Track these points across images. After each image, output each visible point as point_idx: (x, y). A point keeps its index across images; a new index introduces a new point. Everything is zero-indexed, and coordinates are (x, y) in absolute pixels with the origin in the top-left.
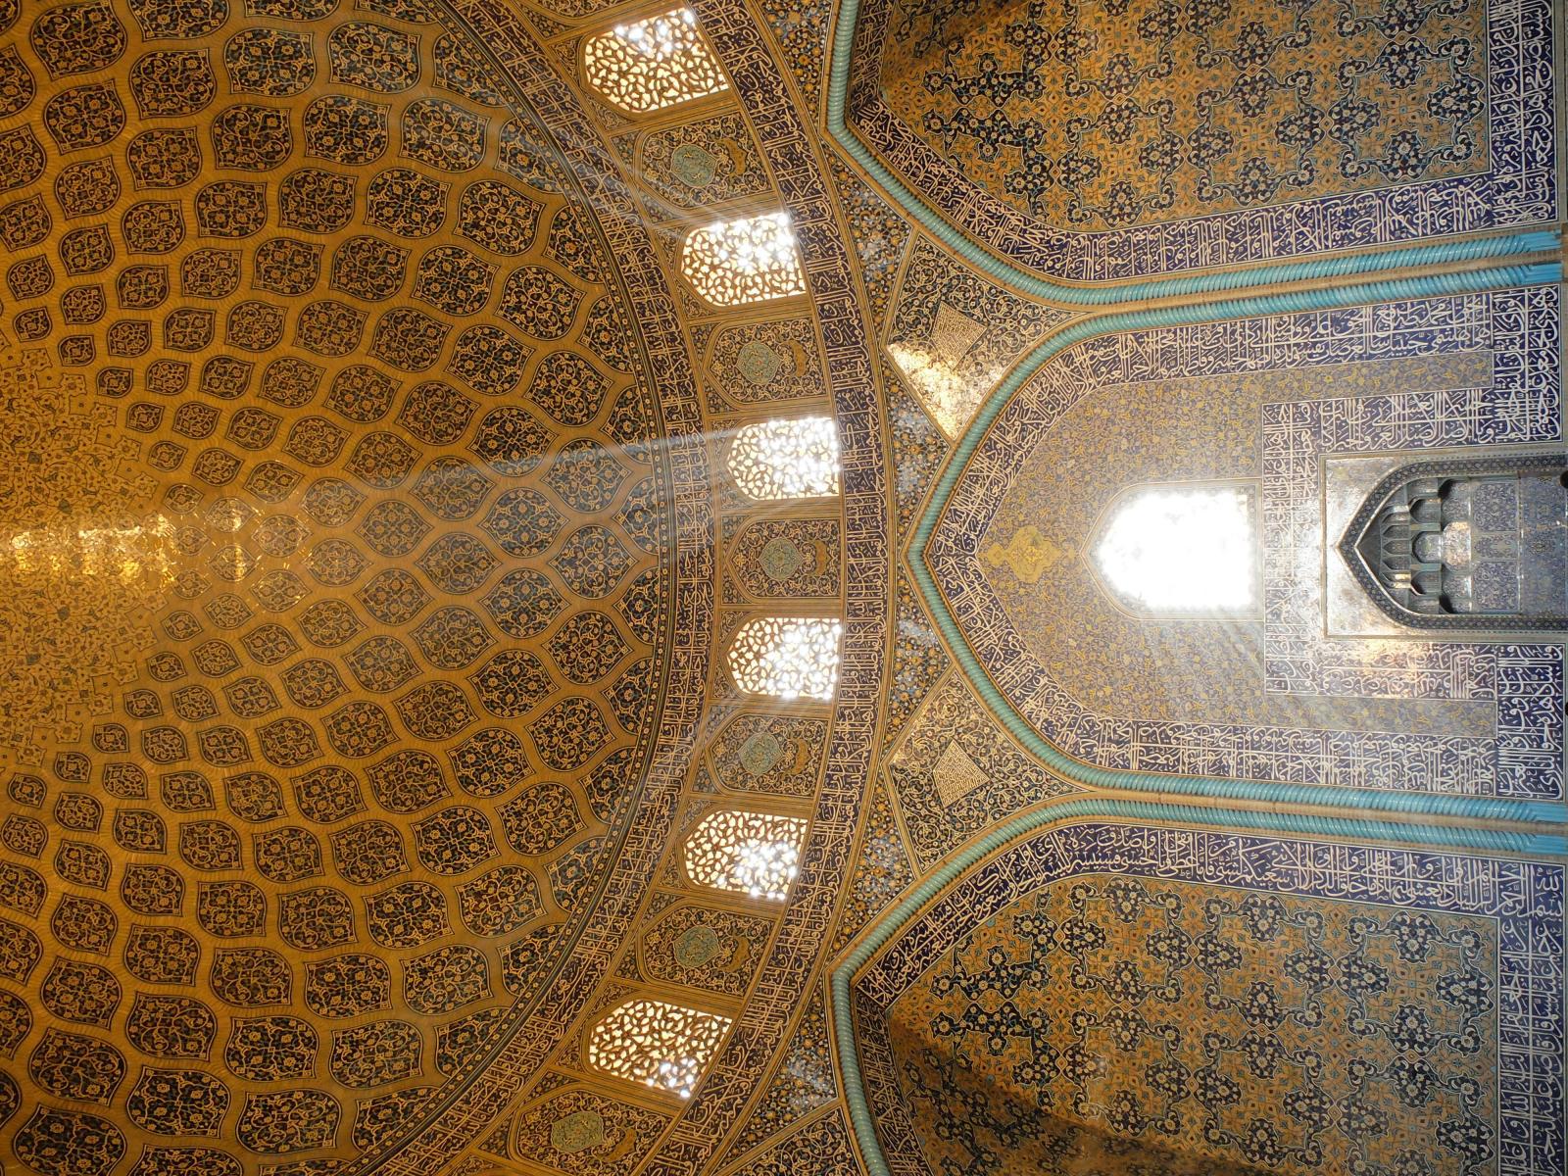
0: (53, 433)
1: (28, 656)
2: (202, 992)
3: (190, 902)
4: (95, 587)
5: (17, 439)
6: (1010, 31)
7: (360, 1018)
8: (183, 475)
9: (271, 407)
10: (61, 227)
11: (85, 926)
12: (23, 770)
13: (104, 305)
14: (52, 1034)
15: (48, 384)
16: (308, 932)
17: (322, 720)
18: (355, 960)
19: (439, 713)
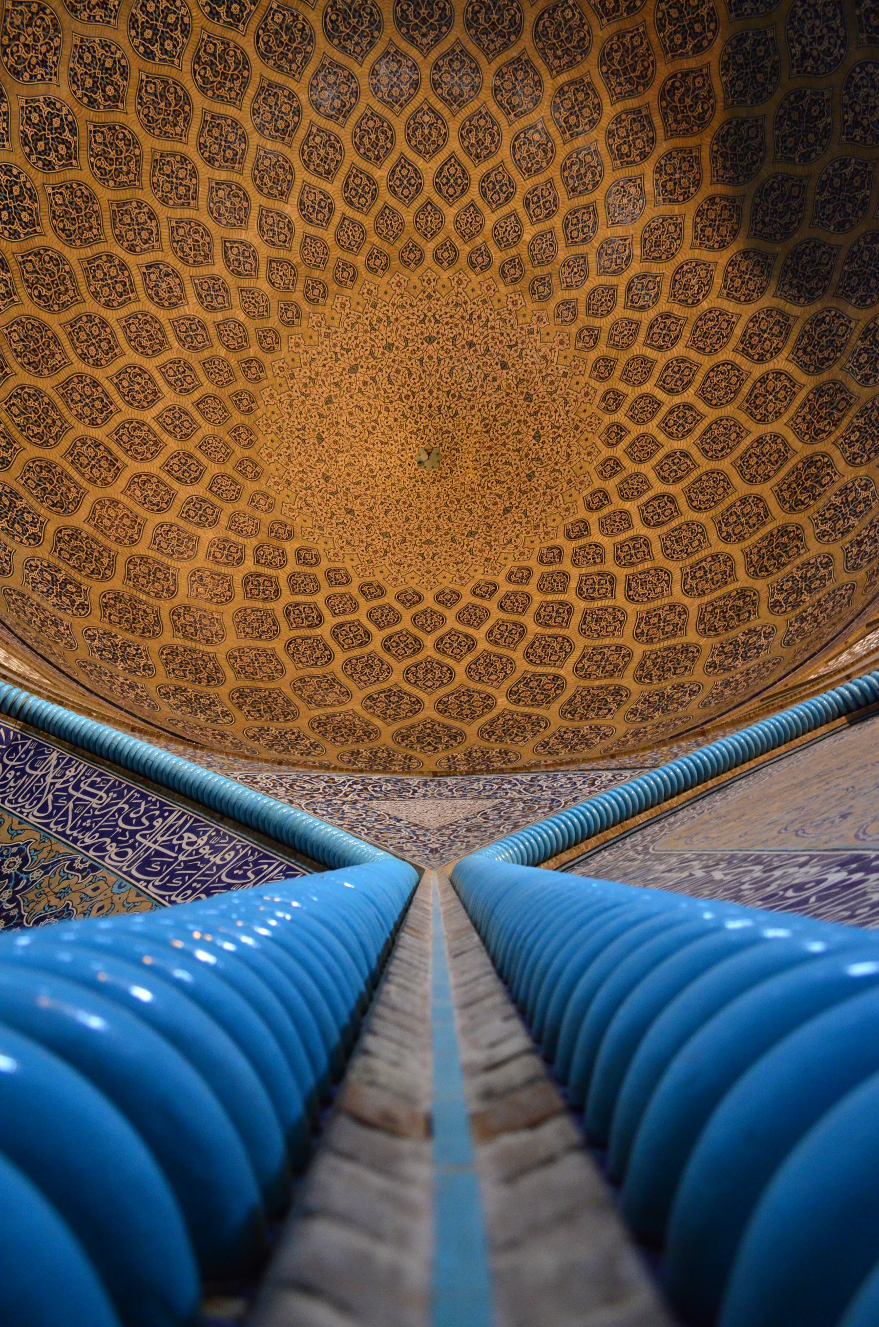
0: (386, 552)
1: (332, 402)
2: (199, 100)
3: (203, 192)
4: (308, 460)
5: (404, 541)
8: (290, 547)
9: (260, 605)
10: (483, 645)
11: (273, 174)
12: (320, 309)
13: (416, 626)
14: (297, 76)
15: (410, 575)
16: (121, 144)
17: (123, 354)
18: (92, 102)
19: (32, 345)
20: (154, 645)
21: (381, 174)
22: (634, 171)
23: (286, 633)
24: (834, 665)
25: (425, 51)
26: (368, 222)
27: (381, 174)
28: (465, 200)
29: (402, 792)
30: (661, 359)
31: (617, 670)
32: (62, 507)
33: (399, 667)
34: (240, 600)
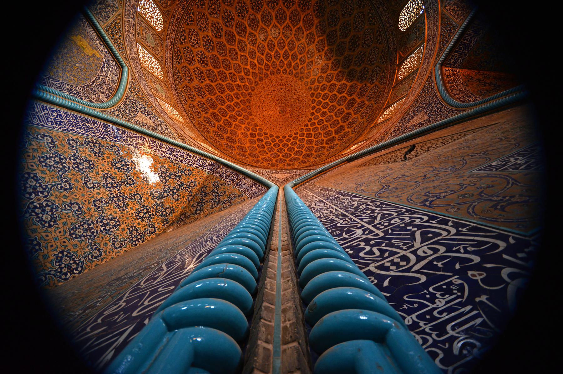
3: (239, 57)
6: (173, 211)
7: (215, 20)
8: (258, 128)
10: (290, 145)
20: (235, 146)
21: (272, 54)
22: (321, 53)
23: (257, 143)
24: (347, 151)
25: (281, 25)
26: (270, 64)
27: (272, 54)
28: (288, 60)
29: (276, 173)
30: (323, 93)
31: (312, 150)
32: (218, 121)
33: (276, 149)
34: (249, 138)
